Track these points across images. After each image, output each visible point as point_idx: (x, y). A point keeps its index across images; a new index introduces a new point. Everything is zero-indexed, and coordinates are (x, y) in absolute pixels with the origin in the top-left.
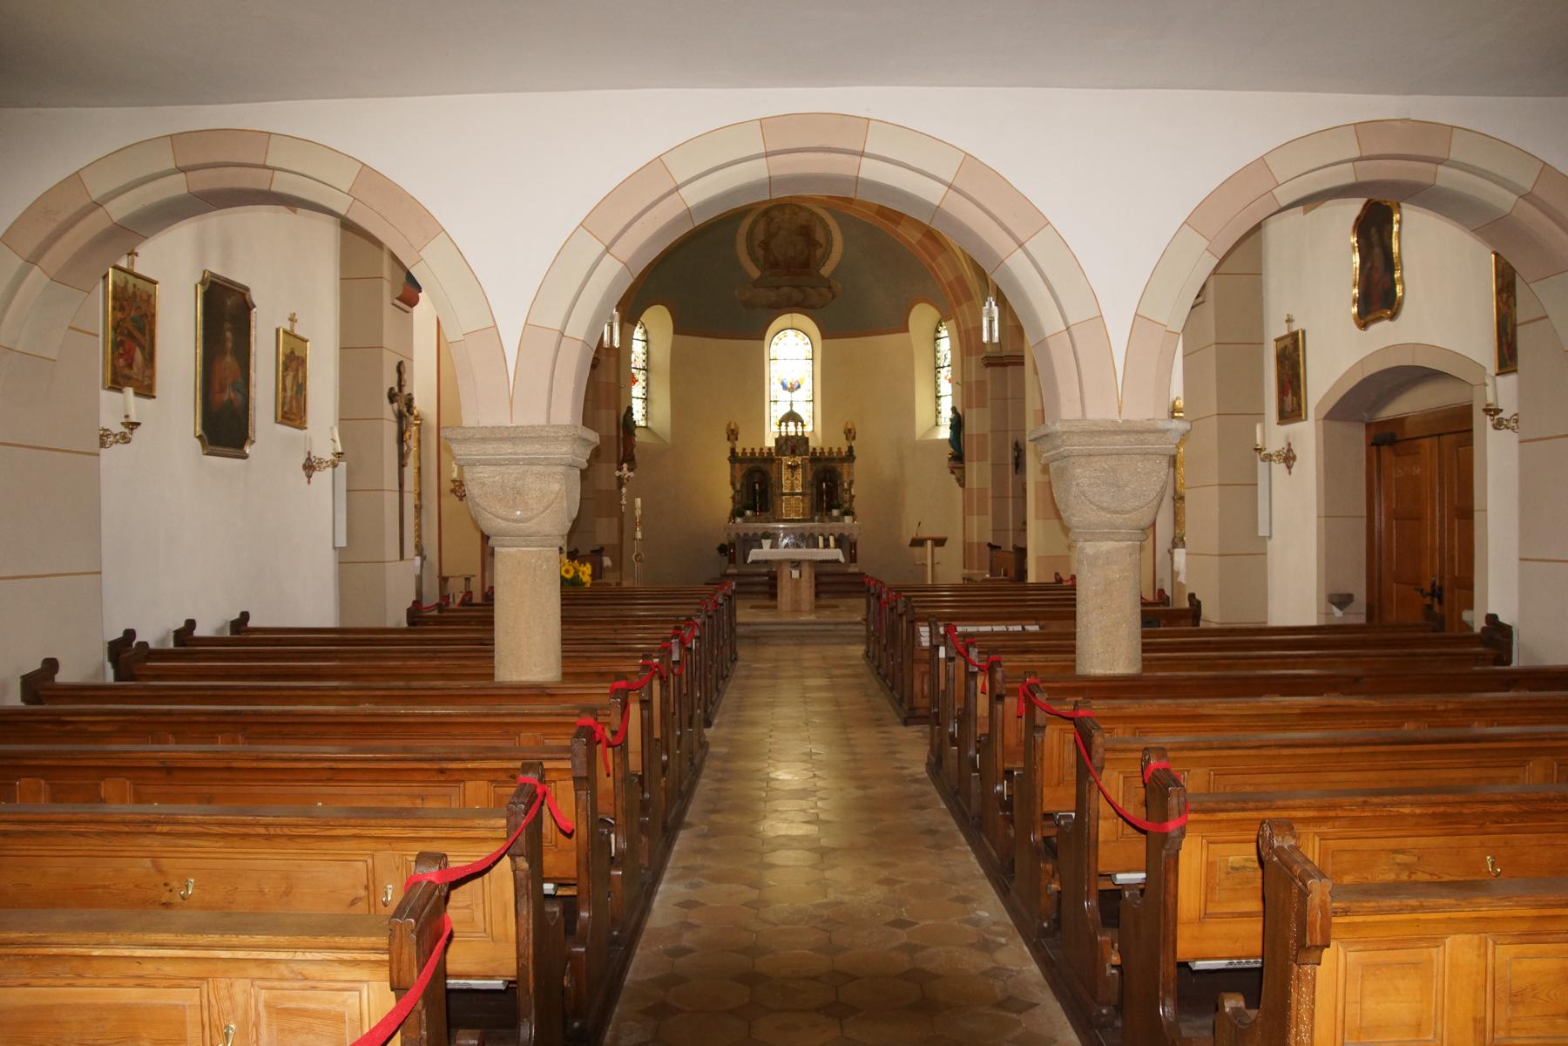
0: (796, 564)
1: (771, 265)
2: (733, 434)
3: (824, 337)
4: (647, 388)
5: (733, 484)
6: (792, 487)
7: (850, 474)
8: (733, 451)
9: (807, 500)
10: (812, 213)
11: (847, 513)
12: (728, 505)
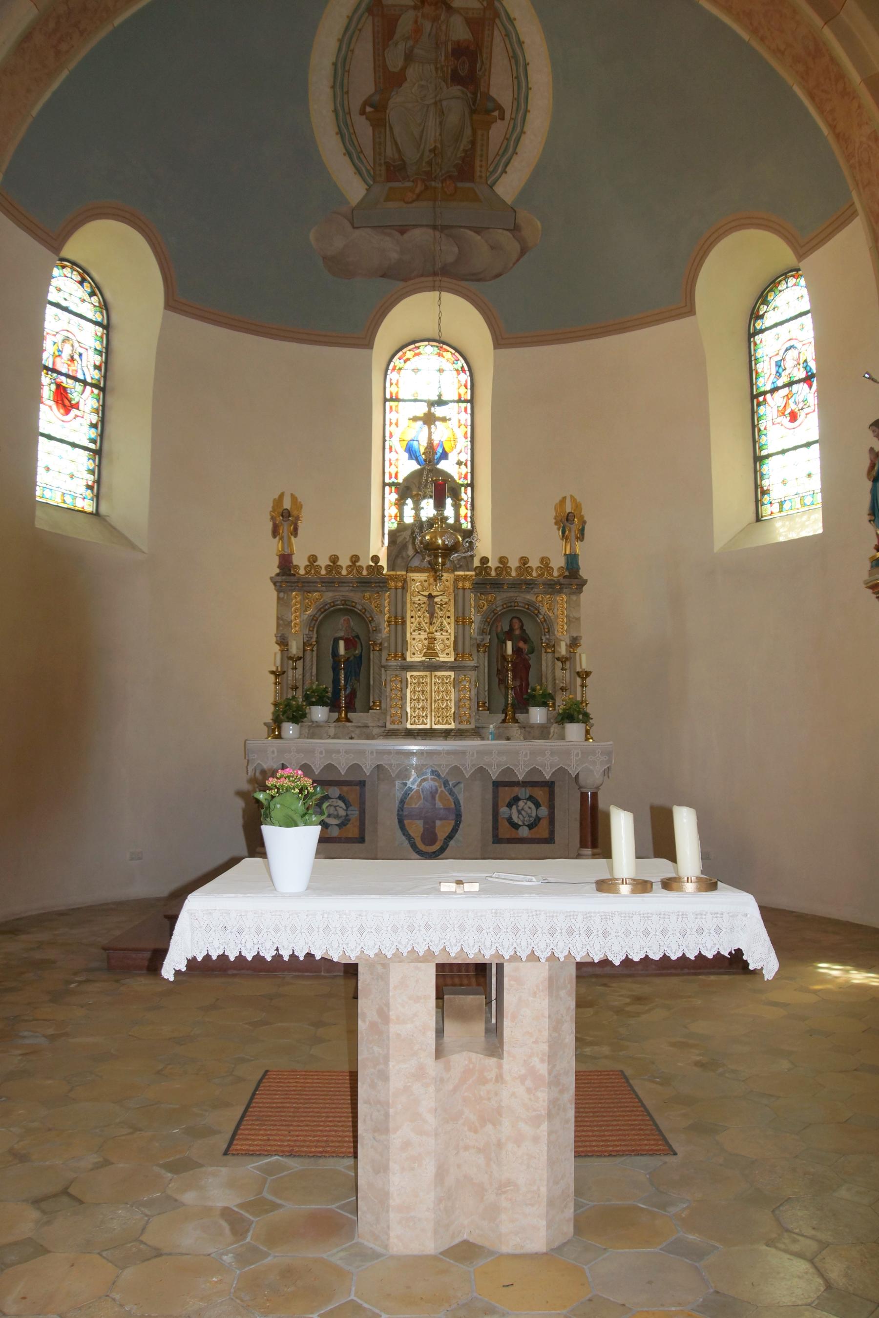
0: (467, 984)
1: (391, 171)
2: (285, 520)
3: (499, 342)
4: (102, 425)
5: (283, 642)
6: (430, 651)
7: (574, 621)
8: (286, 562)
9: (469, 680)
11: (574, 714)
12: (264, 697)
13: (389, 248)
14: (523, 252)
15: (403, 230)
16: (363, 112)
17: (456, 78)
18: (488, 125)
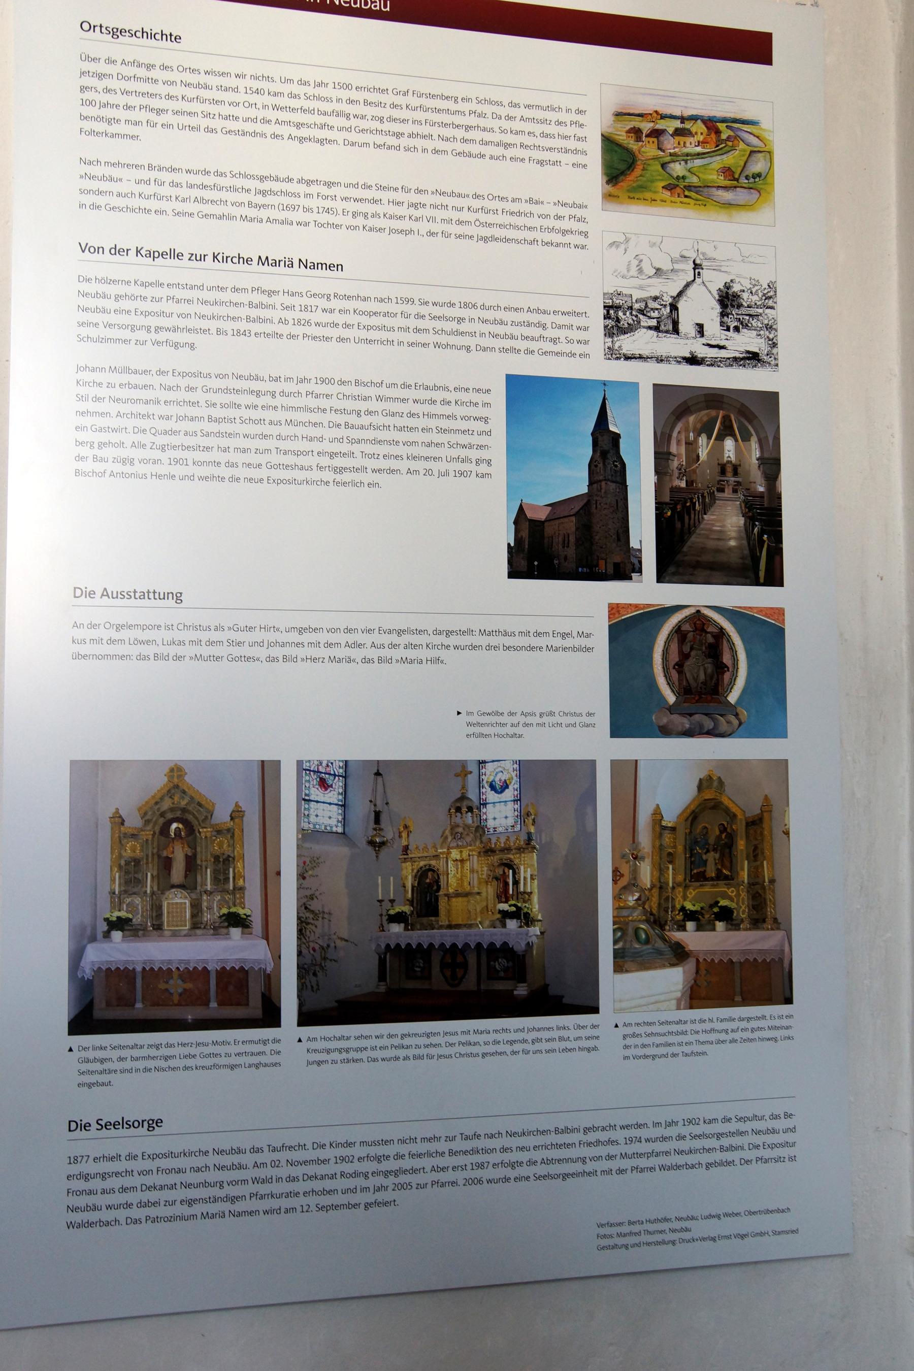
1: (685, 691)
10: (721, 633)
13: (686, 723)
14: (740, 724)
15: (691, 715)
16: (674, 668)
17: (709, 656)
18: (723, 673)
